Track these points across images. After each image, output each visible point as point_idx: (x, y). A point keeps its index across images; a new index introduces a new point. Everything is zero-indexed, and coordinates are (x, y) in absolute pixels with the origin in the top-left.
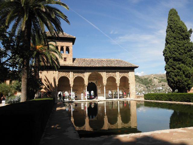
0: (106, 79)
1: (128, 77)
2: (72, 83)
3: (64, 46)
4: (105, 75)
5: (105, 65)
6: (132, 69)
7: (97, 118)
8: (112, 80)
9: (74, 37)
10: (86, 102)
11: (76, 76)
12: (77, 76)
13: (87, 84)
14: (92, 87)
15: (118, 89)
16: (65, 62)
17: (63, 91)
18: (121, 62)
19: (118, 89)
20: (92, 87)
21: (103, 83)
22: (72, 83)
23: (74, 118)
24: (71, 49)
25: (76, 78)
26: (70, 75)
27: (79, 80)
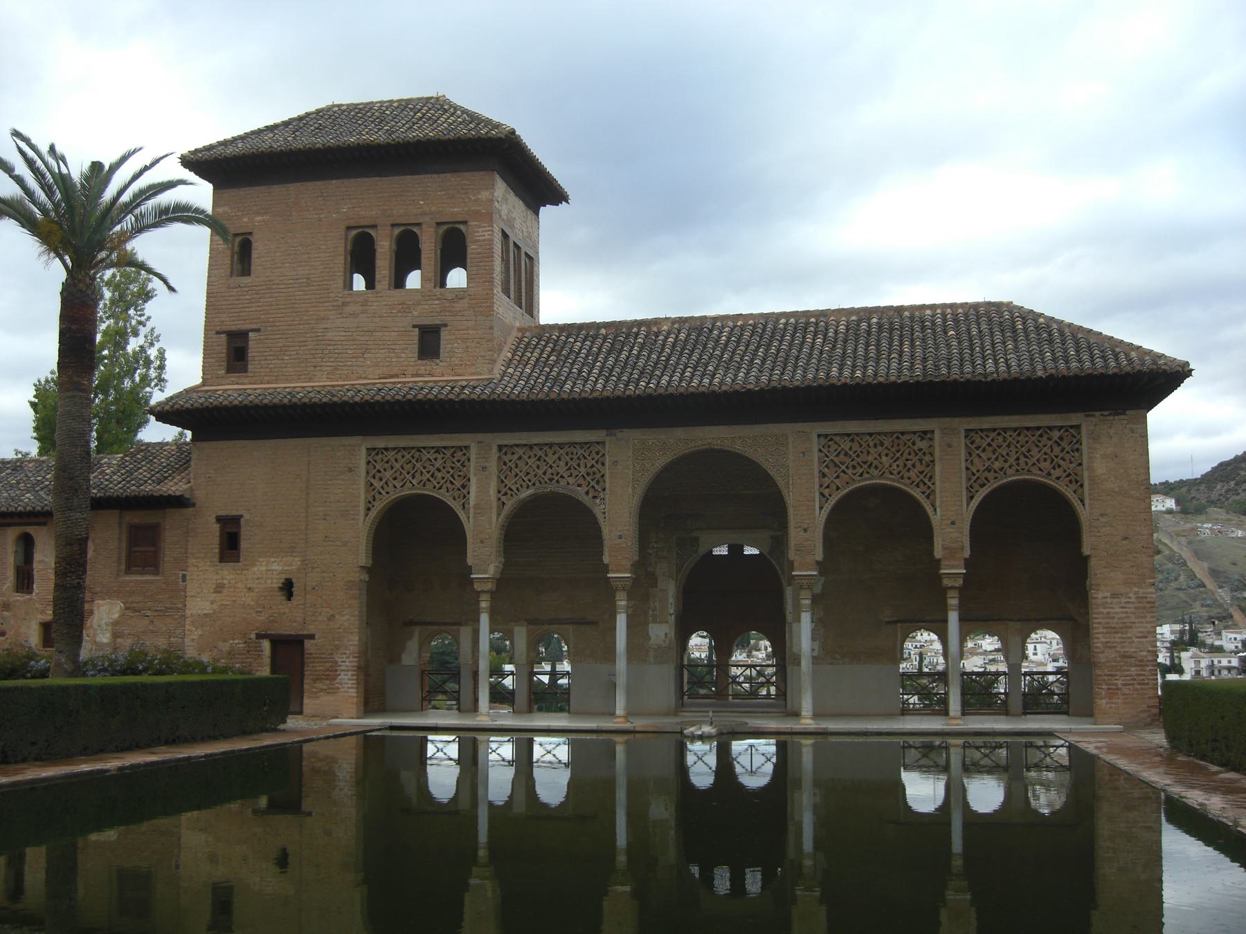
0: (821, 517)
1: (1061, 487)
3: (419, 225)
4: (806, 474)
5: (797, 377)
8: (879, 524)
10: (619, 739)
11: (525, 494)
12: (531, 491)
13: (628, 564)
16: (428, 365)
21: (792, 555)
22: (484, 559)
24: (481, 237)
26: (473, 488)
27: (550, 531)
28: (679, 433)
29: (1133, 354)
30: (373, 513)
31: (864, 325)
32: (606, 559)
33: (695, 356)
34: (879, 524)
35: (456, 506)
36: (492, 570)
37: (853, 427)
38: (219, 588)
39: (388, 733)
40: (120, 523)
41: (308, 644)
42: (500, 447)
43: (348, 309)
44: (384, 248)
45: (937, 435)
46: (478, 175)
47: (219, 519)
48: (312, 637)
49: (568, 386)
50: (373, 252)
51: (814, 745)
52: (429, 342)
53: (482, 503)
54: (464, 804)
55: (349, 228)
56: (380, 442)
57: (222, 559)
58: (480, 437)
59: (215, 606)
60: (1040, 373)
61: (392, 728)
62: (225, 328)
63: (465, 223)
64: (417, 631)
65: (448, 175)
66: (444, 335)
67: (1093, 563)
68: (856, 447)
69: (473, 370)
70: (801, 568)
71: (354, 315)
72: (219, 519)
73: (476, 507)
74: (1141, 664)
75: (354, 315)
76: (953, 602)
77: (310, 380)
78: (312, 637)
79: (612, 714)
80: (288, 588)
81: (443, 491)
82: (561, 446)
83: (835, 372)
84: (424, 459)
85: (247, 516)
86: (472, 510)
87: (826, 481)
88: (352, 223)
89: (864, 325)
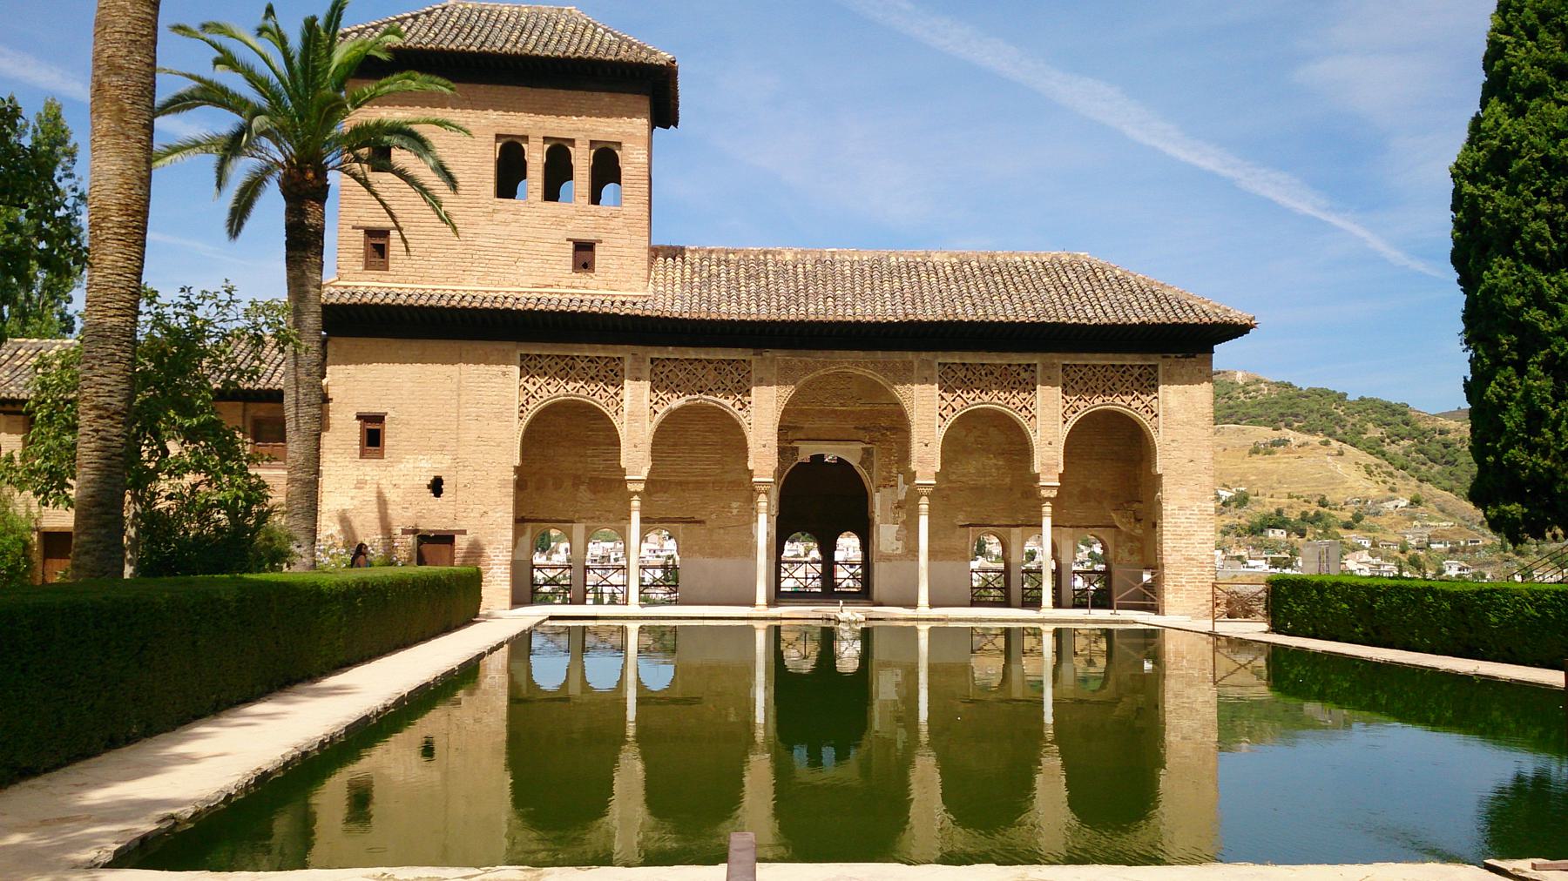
0: (940, 434)
2: (636, 461)
3: (572, 142)
5: (930, 313)
6: (1188, 343)
7: (865, 769)
8: (991, 442)
9: (663, 57)
14: (822, 501)
15: (1047, 522)
16: (582, 278)
17: (579, 530)
18: (1092, 274)
19: (1047, 522)
20: (822, 501)
21: (914, 466)
22: (636, 461)
23: (645, 758)
24: (632, 160)
25: (673, 415)
28: (821, 356)
29: (1205, 307)
30: (528, 417)
31: (967, 269)
32: (751, 466)
33: (830, 287)
34: (991, 442)
35: (610, 412)
36: (644, 475)
37: (971, 358)
38: (360, 485)
39: (548, 623)
40: (244, 417)
41: (457, 538)
42: (652, 361)
43: (498, 217)
44: (535, 158)
45: (1039, 368)
46: (629, 97)
47: (359, 417)
48: (464, 532)
49: (724, 308)
50: (524, 164)
51: (931, 630)
52: (584, 254)
53: (636, 410)
54: (575, 689)
55: (498, 137)
56: (535, 350)
57: (362, 456)
58: (635, 349)
59: (355, 502)
60: (1135, 320)
61: (552, 618)
62: (361, 224)
63: (619, 144)
64: (529, 526)
65: (603, 94)
66: (598, 249)
67: (1164, 479)
68: (970, 374)
69: (627, 286)
70: (923, 476)
71: (506, 223)
72: (363, 418)
73: (631, 414)
74: (1202, 565)
75: (506, 223)
76: (1047, 509)
77: (459, 283)
78: (464, 532)
79: (752, 603)
80: (436, 487)
81: (597, 397)
82: (709, 362)
83: (959, 310)
84: (578, 367)
85: (391, 414)
86: (626, 418)
87: (944, 404)
88: (503, 131)
89: (967, 269)
